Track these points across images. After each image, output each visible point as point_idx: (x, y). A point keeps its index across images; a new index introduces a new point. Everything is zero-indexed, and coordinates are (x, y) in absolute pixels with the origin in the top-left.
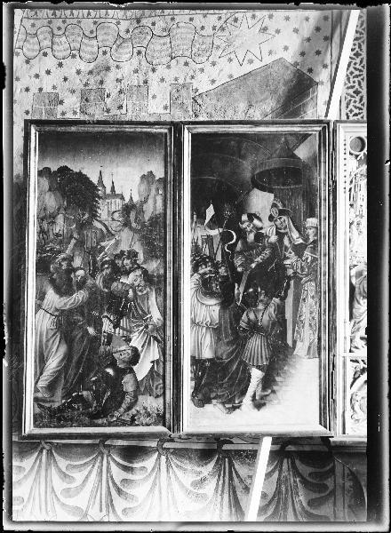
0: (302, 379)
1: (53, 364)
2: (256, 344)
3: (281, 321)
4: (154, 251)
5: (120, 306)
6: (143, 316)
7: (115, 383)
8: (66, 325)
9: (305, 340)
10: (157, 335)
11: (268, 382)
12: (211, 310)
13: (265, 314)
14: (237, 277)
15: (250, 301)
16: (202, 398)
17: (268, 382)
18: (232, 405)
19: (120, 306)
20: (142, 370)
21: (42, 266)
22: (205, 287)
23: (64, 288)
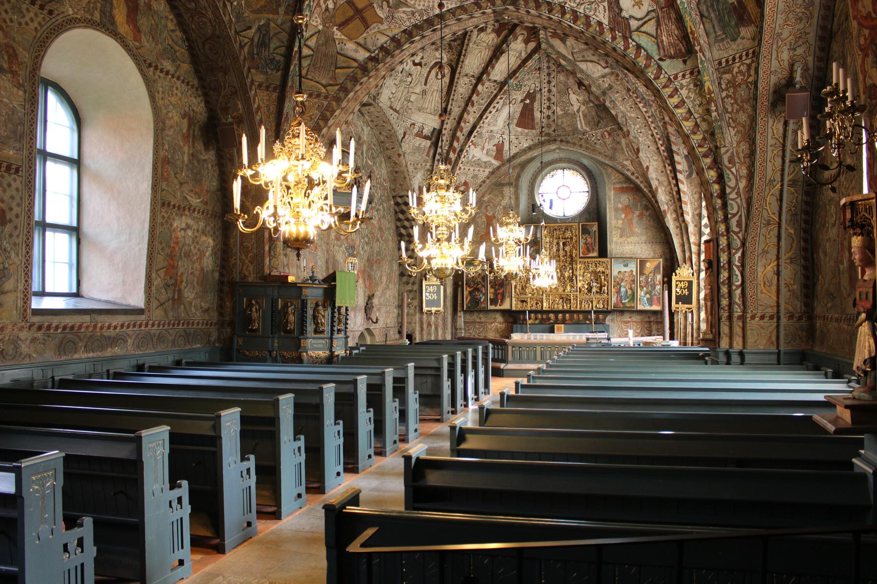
0: (507, 301)
1: (468, 299)
2: (499, 296)
3: (503, 292)
4: (484, 281)
5: (478, 290)
6: (482, 292)
7: (478, 302)
8: (470, 293)
9: (507, 295)
10: (484, 294)
11: (501, 302)
12: (493, 290)
13: (501, 291)
14: (496, 285)
15: (498, 289)
16: (491, 304)
17: (501, 302)
18: (496, 305)
19: (478, 290)
20: (482, 300)
21: (466, 284)
22: (491, 287)
23: (470, 287)
